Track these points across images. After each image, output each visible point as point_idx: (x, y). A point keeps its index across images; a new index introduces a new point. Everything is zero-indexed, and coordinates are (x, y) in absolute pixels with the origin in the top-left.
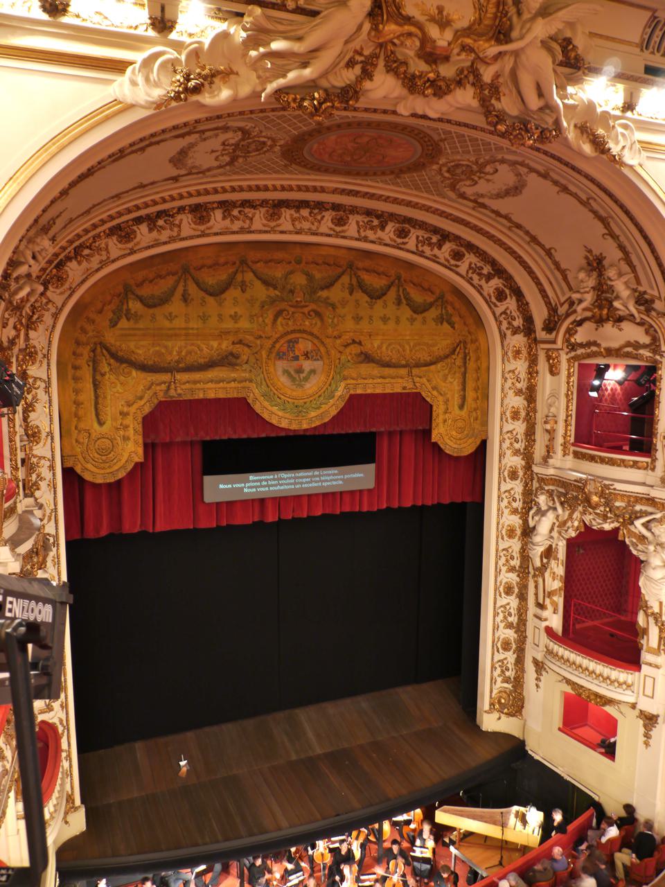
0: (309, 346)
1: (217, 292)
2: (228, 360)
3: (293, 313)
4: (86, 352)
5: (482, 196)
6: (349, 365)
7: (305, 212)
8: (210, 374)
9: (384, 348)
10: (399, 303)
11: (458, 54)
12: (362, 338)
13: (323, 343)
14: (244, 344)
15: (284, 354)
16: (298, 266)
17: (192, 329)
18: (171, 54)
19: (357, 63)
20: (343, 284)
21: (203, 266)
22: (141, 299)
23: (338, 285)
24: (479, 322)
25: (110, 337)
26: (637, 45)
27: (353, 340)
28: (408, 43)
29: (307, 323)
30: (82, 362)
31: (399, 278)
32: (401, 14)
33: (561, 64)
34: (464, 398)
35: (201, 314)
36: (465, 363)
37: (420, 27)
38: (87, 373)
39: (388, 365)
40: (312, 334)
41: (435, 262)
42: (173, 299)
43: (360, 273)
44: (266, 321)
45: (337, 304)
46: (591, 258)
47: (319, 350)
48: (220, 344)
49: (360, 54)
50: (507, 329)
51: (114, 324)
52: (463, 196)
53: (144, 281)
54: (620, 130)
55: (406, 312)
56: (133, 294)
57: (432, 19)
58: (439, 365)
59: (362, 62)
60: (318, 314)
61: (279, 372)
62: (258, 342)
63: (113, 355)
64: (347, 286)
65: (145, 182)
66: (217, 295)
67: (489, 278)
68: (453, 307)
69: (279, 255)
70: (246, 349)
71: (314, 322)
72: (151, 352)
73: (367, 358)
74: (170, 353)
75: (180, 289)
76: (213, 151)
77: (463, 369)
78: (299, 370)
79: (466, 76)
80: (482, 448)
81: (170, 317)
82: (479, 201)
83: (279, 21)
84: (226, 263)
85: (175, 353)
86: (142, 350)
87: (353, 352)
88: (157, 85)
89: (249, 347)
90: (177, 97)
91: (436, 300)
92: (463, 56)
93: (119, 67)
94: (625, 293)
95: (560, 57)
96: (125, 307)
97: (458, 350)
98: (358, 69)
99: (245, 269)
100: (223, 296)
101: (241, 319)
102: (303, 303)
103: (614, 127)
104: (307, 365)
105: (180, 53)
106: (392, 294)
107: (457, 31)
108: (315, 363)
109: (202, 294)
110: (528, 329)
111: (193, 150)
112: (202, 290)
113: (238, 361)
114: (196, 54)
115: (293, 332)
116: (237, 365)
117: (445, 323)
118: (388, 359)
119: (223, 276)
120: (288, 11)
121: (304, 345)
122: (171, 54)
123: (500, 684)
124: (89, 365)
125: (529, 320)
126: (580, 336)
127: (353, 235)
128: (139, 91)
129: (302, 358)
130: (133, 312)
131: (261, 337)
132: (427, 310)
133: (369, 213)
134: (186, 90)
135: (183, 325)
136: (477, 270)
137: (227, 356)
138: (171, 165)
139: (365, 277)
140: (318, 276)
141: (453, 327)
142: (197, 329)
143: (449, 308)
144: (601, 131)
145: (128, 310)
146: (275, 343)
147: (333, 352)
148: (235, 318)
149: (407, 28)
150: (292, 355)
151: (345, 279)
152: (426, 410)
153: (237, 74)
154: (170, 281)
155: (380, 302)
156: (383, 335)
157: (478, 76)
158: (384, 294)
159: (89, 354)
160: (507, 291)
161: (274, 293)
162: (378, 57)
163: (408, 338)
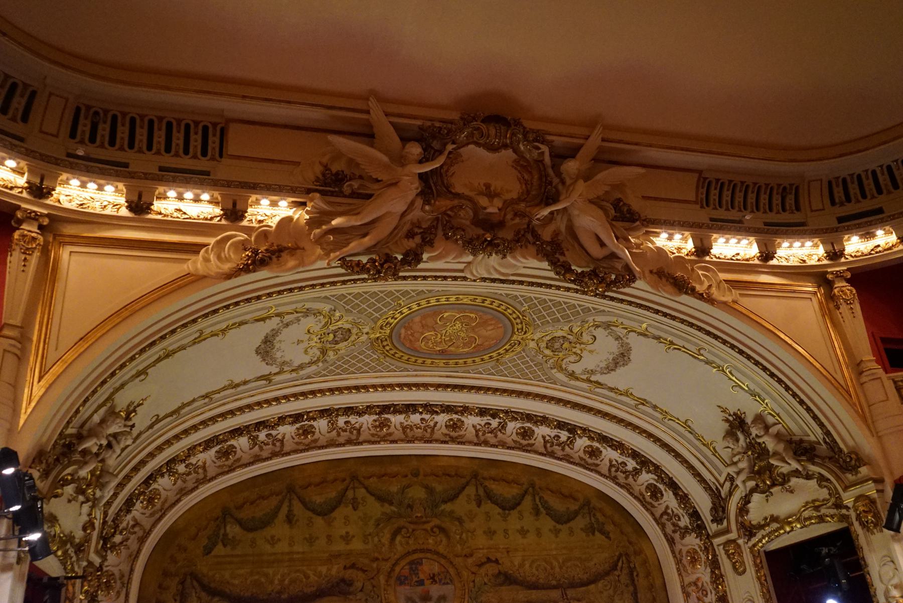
0: (436, 569)
1: (326, 511)
3: (413, 530)
4: (173, 584)
5: (593, 372)
6: (486, 588)
9: (527, 566)
10: (537, 513)
11: (512, 219)
12: (498, 555)
13: (451, 563)
14: (358, 569)
15: (406, 578)
16: (415, 479)
17: (298, 553)
18: (242, 236)
19: (417, 234)
20: (468, 496)
21: (309, 485)
22: (240, 523)
23: (462, 498)
25: (203, 567)
26: (696, 202)
27: (488, 559)
28: (462, 213)
29: (431, 541)
31: (533, 485)
32: (451, 192)
33: (615, 219)
35: (308, 536)
36: (633, 580)
37: (470, 199)
40: (437, 553)
42: (276, 521)
43: (486, 483)
44: (383, 540)
45: (465, 518)
46: (731, 418)
47: (448, 572)
48: (329, 570)
49: (420, 227)
50: (674, 532)
51: (208, 551)
52: (572, 375)
53: (244, 504)
54: (700, 272)
55: (547, 523)
56: (232, 516)
57: (481, 193)
58: (600, 584)
59: (421, 233)
60: (442, 530)
62: (375, 565)
63: (205, 588)
64: (473, 497)
65: (237, 381)
66: (326, 515)
69: (394, 469)
70: (360, 574)
71: (439, 539)
72: (248, 582)
74: (272, 582)
75: (284, 510)
76: (299, 342)
77: (631, 588)
79: (523, 235)
81: (273, 541)
82: (592, 379)
83: (340, 204)
84: (335, 480)
85: (276, 582)
87: (490, 573)
88: (228, 260)
89: (364, 571)
91: (581, 508)
92: (517, 220)
93: (194, 249)
95: (612, 212)
96: (222, 531)
97: (620, 564)
98: (418, 239)
99: (356, 485)
100: (333, 515)
101: (354, 539)
102: (424, 519)
103: (693, 270)
105: (250, 236)
106: (527, 502)
107: (505, 201)
108: (445, 587)
109: (310, 514)
111: (278, 339)
112: (309, 509)
113: (352, 589)
114: (265, 235)
115: (415, 551)
116: (350, 593)
117: (596, 533)
118: (534, 579)
119: (332, 494)
120: (345, 196)
121: (429, 567)
122: (242, 236)
124: (175, 600)
125: (695, 515)
129: (427, 582)
130: (230, 536)
131: (377, 559)
132: (573, 519)
134: (254, 263)
135: (287, 549)
137: (338, 583)
138: (258, 358)
140: (439, 488)
141: (608, 538)
142: (303, 553)
143: (598, 515)
144: (679, 274)
145: (225, 535)
146: (394, 565)
147: (465, 573)
149: (456, 202)
150: (415, 579)
151: (470, 490)
153: (303, 249)
155: (515, 513)
156: (524, 550)
157: (537, 237)
158: (519, 504)
160: (661, 487)
161: (388, 509)
162: (436, 228)
163: (554, 553)
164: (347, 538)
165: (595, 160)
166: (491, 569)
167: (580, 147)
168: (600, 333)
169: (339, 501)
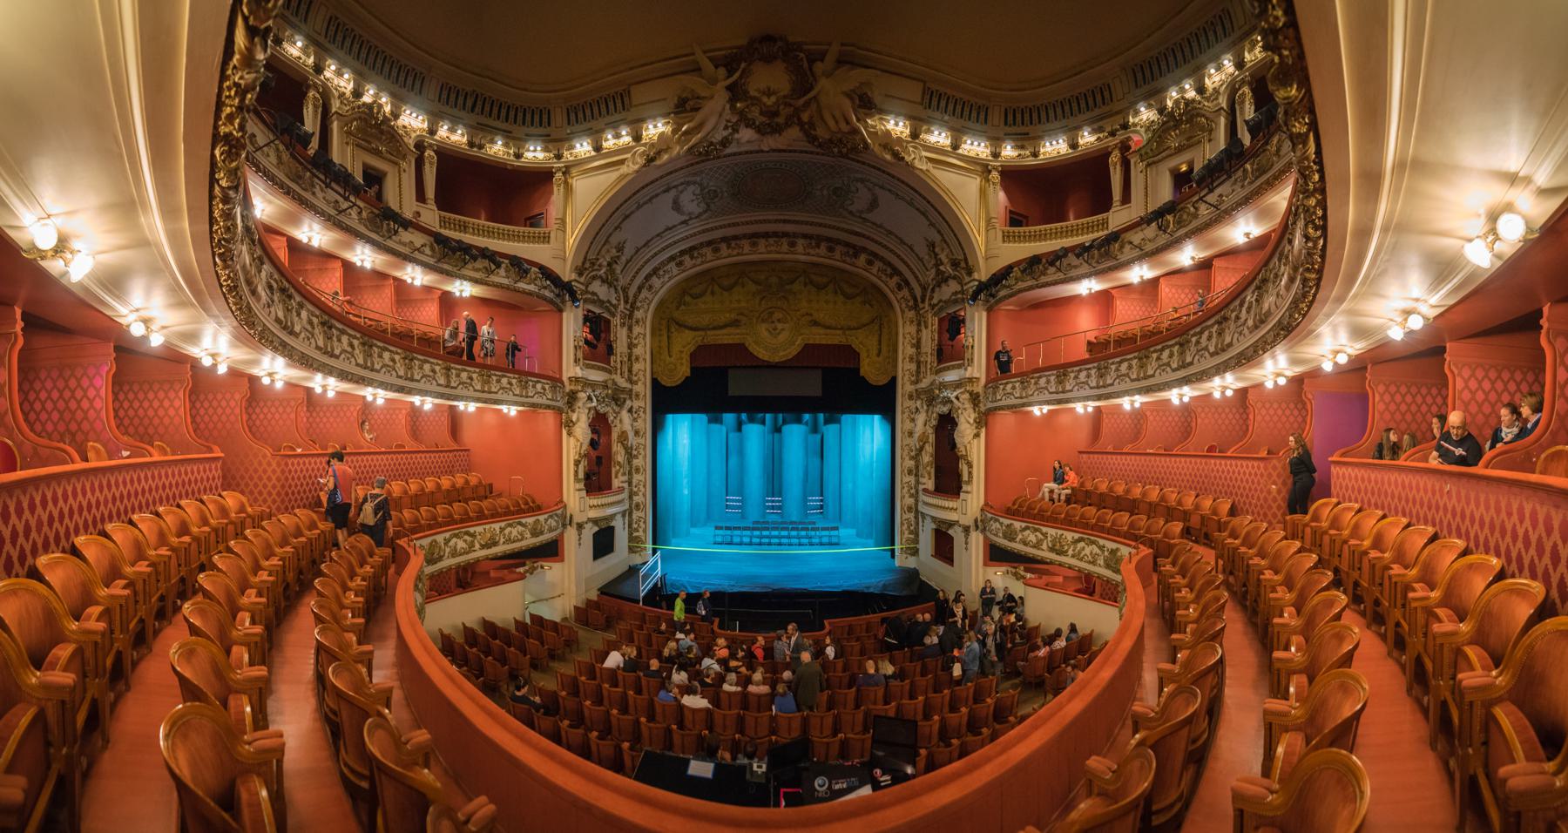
1: (729, 289)
2: (735, 323)
8: (724, 331)
24: (890, 304)
25: (676, 315)
38: (665, 332)
39: (829, 328)
61: (763, 330)
67: (891, 276)
68: (872, 295)
73: (816, 323)
80: (894, 379)
86: (690, 320)
94: (945, 260)
104: (780, 326)
114: (653, 145)
123: (906, 535)
126: (935, 301)
127: (801, 254)
148: (739, 301)
152: (856, 355)
159: (667, 322)
169: (736, 283)
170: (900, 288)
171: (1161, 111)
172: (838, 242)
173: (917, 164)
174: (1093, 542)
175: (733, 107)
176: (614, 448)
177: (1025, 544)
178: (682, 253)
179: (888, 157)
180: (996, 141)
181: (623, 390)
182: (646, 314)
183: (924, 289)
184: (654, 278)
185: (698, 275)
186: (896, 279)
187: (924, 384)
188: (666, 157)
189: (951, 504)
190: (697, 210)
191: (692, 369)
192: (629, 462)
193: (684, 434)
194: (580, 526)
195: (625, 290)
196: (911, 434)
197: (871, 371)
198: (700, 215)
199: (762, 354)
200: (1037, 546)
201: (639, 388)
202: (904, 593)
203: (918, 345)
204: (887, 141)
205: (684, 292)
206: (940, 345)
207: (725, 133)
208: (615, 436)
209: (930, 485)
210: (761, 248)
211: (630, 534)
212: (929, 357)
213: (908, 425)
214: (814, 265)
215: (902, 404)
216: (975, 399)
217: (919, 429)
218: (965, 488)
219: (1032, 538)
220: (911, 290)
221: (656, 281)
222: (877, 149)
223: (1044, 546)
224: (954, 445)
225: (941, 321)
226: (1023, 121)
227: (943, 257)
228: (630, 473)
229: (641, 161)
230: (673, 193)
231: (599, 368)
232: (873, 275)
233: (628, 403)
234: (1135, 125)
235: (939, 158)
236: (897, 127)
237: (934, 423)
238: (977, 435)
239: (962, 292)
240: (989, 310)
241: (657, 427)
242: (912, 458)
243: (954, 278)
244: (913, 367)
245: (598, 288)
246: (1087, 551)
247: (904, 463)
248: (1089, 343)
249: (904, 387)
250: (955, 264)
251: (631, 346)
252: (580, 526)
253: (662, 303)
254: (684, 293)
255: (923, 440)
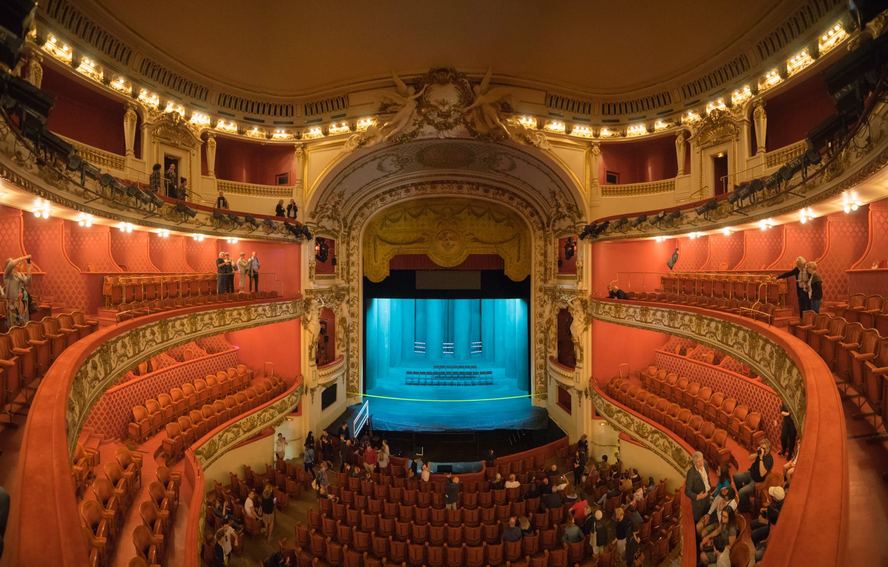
2: (420, 240)
4: (372, 238)
7: (445, 185)
8: (413, 246)
18: (357, 135)
25: (380, 233)
30: (371, 241)
34: (519, 258)
38: (372, 245)
41: (503, 201)
61: (440, 245)
73: (476, 240)
78: (448, 245)
80: (529, 277)
86: (391, 238)
90: (358, 147)
104: (451, 243)
110: (543, 228)
114: (364, 134)
121: (449, 235)
122: (357, 135)
123: (539, 385)
127: (466, 193)
128: (348, 148)
133: (498, 189)
136: (521, 204)
139: (474, 208)
151: (466, 210)
154: (400, 214)
159: (372, 238)
161: (437, 216)
164: (423, 225)
165: (490, 83)
166: (471, 237)
167: (481, 79)
168: (503, 156)
170: (532, 215)
171: (703, 115)
172: (491, 187)
173: (542, 146)
174: (665, 437)
175: (419, 112)
176: (337, 329)
177: (619, 422)
178: (384, 193)
179: (522, 142)
180: (596, 127)
181: (343, 289)
182: (358, 233)
183: (549, 218)
184: (365, 209)
185: (394, 206)
186: (529, 209)
187: (550, 284)
188: (372, 142)
189: (569, 374)
190: (394, 170)
191: (391, 271)
192: (347, 336)
193: (384, 308)
194: (313, 390)
195: (344, 219)
196: (541, 316)
197: (513, 272)
198: (396, 172)
199: (439, 261)
200: (628, 426)
201: (354, 284)
202: (537, 428)
203: (545, 255)
204: (522, 132)
205: (386, 218)
206: (560, 258)
207: (414, 128)
208: (337, 320)
209: (555, 353)
210: (439, 190)
211: (348, 385)
212: (554, 267)
213: (539, 310)
214: (476, 200)
215: (534, 294)
216: (584, 304)
217: (547, 315)
218: (578, 364)
219: (623, 419)
220: (540, 217)
221: (366, 211)
222: (514, 138)
223: (632, 428)
224: (570, 334)
225: (560, 240)
226: (615, 112)
227: (561, 202)
228: (348, 343)
229: (356, 144)
230: (378, 161)
231: (327, 278)
232: (513, 206)
233: (347, 298)
234: (685, 123)
235: (556, 140)
236: (528, 122)
237: (557, 313)
238: (586, 329)
239: (574, 227)
240: (593, 243)
241: (367, 306)
242: (542, 332)
243: (569, 217)
244: (542, 269)
245: (327, 224)
246: (661, 441)
247: (536, 335)
248: (662, 278)
249: (536, 284)
250: (570, 208)
251: (349, 256)
252: (313, 390)
253: (370, 225)
254: (387, 217)
255: (549, 321)
